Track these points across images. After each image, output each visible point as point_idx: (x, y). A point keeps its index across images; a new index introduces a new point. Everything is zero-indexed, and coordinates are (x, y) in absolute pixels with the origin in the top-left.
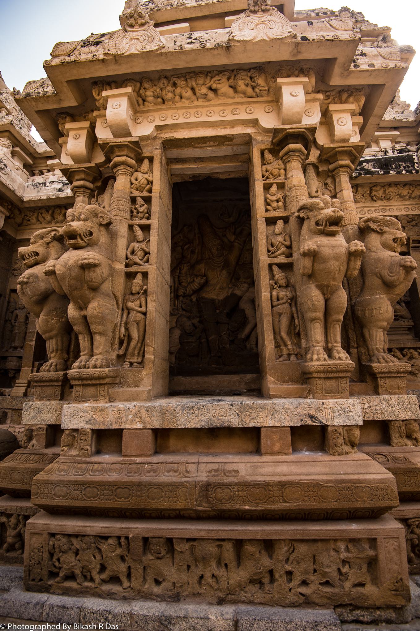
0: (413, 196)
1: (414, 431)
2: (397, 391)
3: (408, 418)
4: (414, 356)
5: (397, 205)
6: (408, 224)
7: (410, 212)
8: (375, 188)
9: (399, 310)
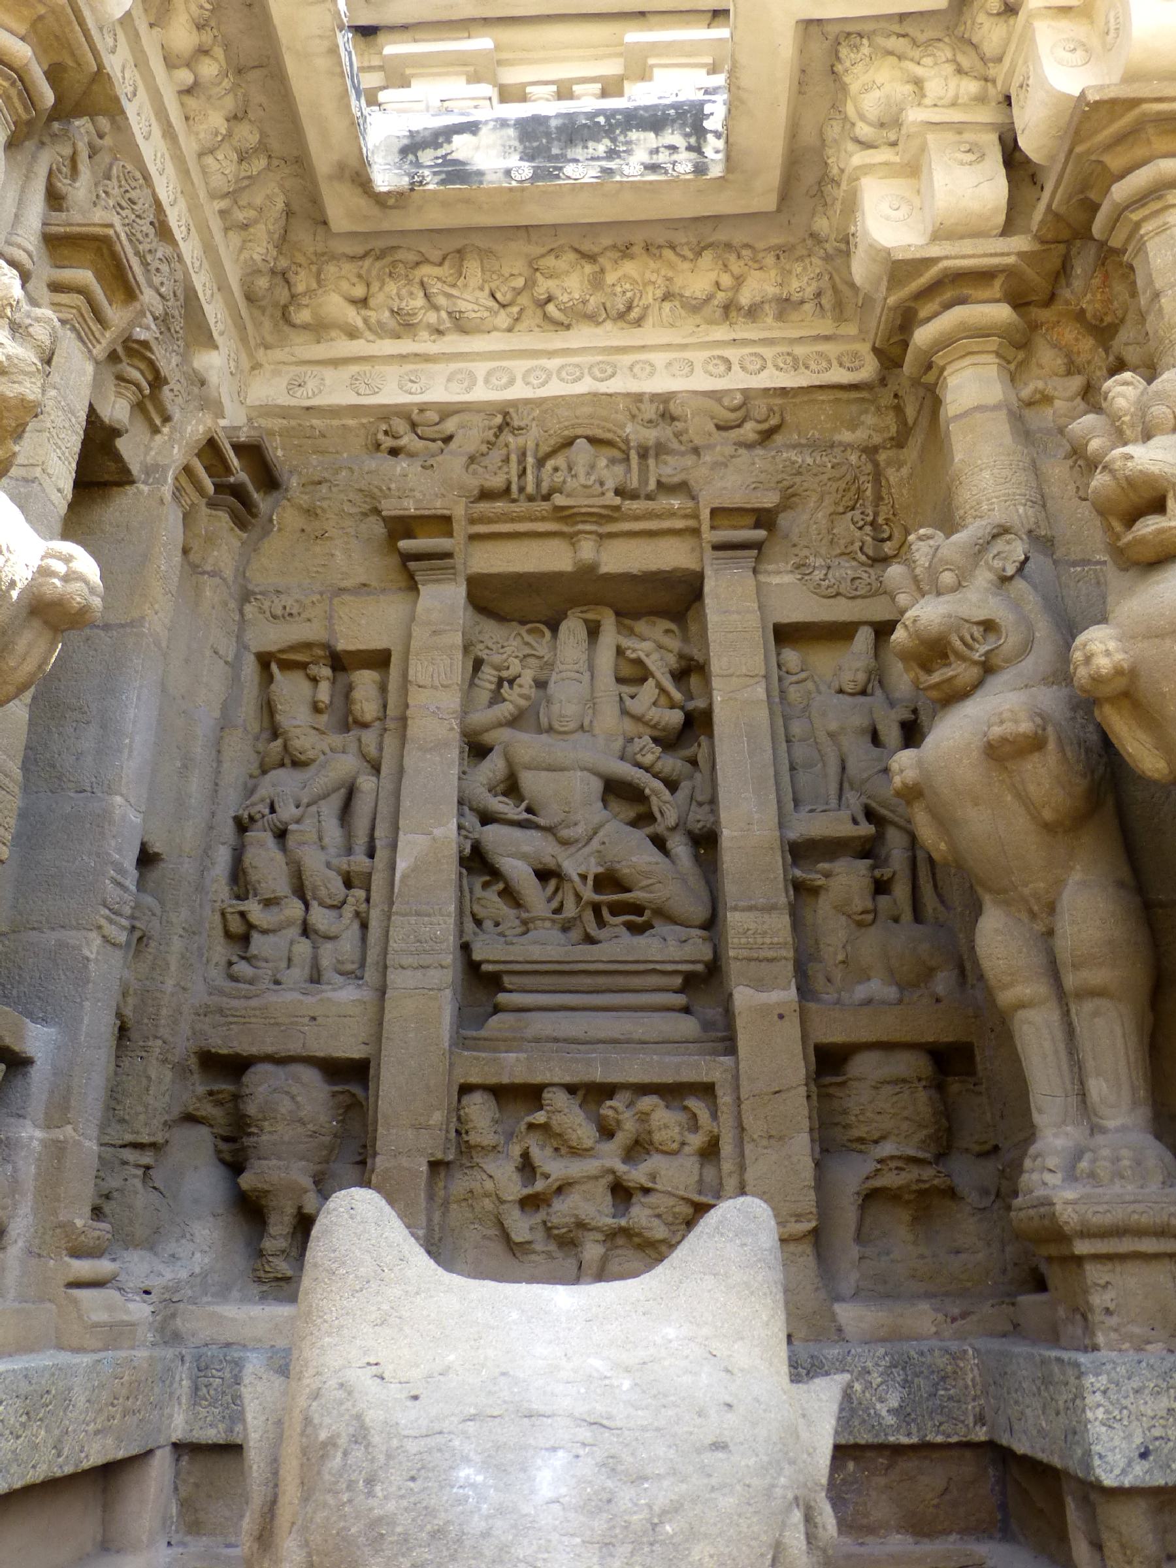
0: (745, 299)
4: (657, 1137)
5: (668, 347)
6: (718, 436)
7: (738, 381)
8: (550, 261)
9: (647, 875)
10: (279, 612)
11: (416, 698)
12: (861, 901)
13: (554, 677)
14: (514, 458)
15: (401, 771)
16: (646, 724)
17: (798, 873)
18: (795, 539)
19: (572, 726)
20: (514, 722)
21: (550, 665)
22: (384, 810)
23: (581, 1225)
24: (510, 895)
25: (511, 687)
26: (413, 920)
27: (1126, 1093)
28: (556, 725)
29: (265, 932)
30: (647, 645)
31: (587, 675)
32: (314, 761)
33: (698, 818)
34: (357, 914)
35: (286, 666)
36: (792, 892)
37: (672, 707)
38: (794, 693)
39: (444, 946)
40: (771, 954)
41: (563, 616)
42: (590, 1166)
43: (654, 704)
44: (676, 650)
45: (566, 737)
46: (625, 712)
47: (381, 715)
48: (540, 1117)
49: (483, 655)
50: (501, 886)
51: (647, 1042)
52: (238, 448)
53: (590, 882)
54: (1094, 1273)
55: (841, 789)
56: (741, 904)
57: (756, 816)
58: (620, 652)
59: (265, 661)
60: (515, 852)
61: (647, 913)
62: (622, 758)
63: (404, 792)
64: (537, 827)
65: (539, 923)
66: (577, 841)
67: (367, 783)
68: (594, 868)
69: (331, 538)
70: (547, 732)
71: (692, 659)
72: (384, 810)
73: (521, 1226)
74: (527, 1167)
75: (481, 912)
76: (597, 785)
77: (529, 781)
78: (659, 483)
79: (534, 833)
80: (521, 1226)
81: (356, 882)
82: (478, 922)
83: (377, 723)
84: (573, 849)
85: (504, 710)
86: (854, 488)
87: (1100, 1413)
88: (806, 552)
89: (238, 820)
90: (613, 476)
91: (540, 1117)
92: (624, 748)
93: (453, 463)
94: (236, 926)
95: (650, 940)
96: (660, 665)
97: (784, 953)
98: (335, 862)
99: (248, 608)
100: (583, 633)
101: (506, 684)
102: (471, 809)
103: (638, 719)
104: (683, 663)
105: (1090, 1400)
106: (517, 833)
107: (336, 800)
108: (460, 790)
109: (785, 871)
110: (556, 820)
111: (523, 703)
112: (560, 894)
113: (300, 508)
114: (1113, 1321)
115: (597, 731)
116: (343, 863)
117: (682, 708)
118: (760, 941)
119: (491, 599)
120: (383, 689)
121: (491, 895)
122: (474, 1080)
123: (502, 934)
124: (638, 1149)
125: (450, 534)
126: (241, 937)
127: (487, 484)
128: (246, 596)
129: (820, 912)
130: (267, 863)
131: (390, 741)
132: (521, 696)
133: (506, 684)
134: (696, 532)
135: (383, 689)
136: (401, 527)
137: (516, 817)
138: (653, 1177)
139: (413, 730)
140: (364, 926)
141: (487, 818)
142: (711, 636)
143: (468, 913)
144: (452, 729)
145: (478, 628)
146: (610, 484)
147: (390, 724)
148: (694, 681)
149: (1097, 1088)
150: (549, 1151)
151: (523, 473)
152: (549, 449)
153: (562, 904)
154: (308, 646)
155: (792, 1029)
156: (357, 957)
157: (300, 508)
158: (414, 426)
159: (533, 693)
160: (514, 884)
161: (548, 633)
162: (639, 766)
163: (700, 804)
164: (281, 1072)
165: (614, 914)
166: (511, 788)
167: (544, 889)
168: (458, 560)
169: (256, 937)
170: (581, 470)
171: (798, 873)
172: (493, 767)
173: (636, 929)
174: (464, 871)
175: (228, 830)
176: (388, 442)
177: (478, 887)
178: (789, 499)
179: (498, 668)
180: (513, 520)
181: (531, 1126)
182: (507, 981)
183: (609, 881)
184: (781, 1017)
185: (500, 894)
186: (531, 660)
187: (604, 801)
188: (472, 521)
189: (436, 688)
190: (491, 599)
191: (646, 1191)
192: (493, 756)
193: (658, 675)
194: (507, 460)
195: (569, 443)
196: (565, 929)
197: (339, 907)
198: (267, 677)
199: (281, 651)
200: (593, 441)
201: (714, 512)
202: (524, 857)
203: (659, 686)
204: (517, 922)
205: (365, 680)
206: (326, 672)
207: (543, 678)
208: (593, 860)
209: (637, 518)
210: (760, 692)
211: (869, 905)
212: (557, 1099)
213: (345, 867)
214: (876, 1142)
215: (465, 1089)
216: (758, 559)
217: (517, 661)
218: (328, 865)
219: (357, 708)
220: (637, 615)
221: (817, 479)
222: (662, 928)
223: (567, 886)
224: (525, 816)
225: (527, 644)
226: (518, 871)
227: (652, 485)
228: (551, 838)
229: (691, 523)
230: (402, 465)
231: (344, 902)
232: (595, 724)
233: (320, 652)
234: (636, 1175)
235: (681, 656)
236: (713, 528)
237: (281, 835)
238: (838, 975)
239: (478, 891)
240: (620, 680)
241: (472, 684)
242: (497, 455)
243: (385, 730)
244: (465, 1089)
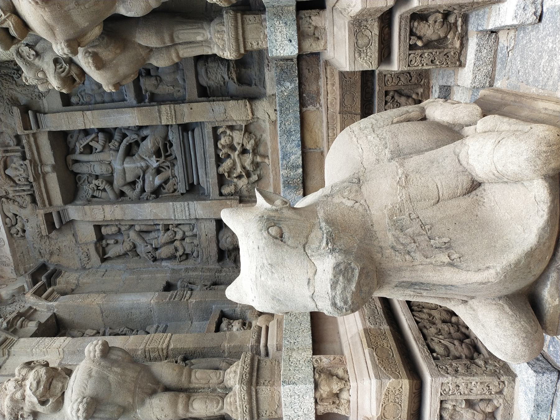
1: (331, 391)
2: (276, 397)
3: (313, 400)
4: (228, 143)
9: (154, 144)
10: (87, 259)
12: (153, 81)
14: (18, 194)
15: (132, 220)
17: (147, 100)
18: (29, 99)
19: (109, 167)
23: (253, 162)
24: (166, 181)
27: (201, 31)
28: (110, 172)
29: (185, 250)
30: (77, 145)
32: (133, 243)
35: (104, 253)
36: (154, 103)
37: (98, 136)
40: (173, 111)
41: (72, 171)
42: (237, 160)
43: (98, 142)
46: (102, 151)
48: (226, 174)
51: (204, 145)
52: (35, 282)
53: (159, 159)
54: (249, 48)
58: (81, 153)
59: (103, 260)
67: (137, 228)
68: (154, 158)
69: (59, 247)
73: (254, 178)
74: (240, 177)
76: (127, 159)
77: (129, 178)
78: (17, 145)
79: (146, 177)
80: (254, 178)
81: (167, 228)
82: (175, 190)
85: (107, 188)
86: (4, 77)
87: (282, 52)
88: (34, 95)
89: (154, 261)
90: (17, 162)
91: (226, 174)
93: (24, 213)
94: (184, 257)
97: (172, 107)
98: (162, 234)
99: (87, 267)
100: (77, 165)
103: (104, 147)
105: (279, 55)
106: (147, 182)
107: (144, 235)
110: (141, 170)
111: (104, 183)
113: (50, 257)
114: (260, 43)
116: (162, 232)
117: (98, 133)
119: (71, 194)
121: (167, 187)
122: (218, 193)
123: (178, 183)
124: (232, 148)
125: (51, 213)
126: (187, 256)
127: (30, 201)
128: (84, 268)
130: (164, 252)
132: (102, 184)
134: (34, 134)
136: (51, 226)
138: (239, 144)
140: (180, 224)
141: (143, 190)
146: (22, 162)
149: (199, 38)
150: (235, 171)
151: (24, 190)
152: (12, 182)
154: (97, 249)
155: (194, 105)
156: (188, 226)
157: (50, 257)
158: (12, 226)
161: (79, 175)
162: (119, 146)
164: (221, 241)
165: (167, 151)
166: (133, 184)
168: (59, 209)
169: (186, 252)
170: (18, 173)
171: (147, 100)
173: (171, 145)
175: (157, 263)
176: (21, 233)
177: (164, 191)
178: (14, 102)
179: (94, 191)
180: (42, 194)
181: (229, 176)
182: (191, 182)
183: (158, 154)
184: (191, 109)
186: (89, 180)
188: (45, 206)
190: (71, 194)
191: (243, 145)
192: (123, 190)
193: (87, 141)
194: (20, 196)
195: (9, 177)
196: (174, 165)
197: (175, 232)
198: (109, 259)
199: (100, 256)
200: (6, 167)
201: (26, 129)
203: (91, 141)
205: (104, 231)
206: (104, 242)
208: (152, 159)
209: (33, 153)
210: (88, 113)
211: (153, 79)
212: (221, 170)
214: (224, 79)
215: (221, 194)
216: (40, 112)
218: (163, 235)
220: (68, 147)
221: (4, 90)
223: (161, 165)
225: (84, 181)
226: (158, 181)
227: (18, 148)
229: (31, 136)
230: (27, 228)
233: (98, 245)
234: (239, 148)
236: (31, 129)
237: (156, 249)
238: (177, 89)
239: (166, 191)
242: (18, 199)
244: (221, 194)
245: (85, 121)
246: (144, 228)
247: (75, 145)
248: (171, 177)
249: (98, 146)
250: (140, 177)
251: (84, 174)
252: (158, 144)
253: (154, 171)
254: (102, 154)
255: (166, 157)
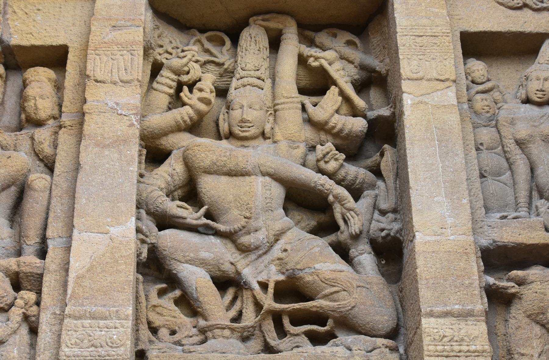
11: (94, 94)
13: (234, 83)
15: (77, 167)
16: (329, 132)
17: (491, 280)
19: (253, 131)
20: (194, 127)
21: (230, 73)
22: (58, 209)
24: (188, 304)
25: (191, 91)
26: (87, 322)
28: (237, 130)
30: (330, 54)
31: (269, 82)
33: (387, 225)
34: (26, 318)
36: (486, 300)
37: (355, 116)
38: (480, 102)
39: (121, 350)
41: (244, 24)
43: (337, 111)
44: (357, 62)
45: (246, 143)
47: (56, 112)
49: (162, 59)
50: (177, 293)
53: (271, 290)
55: (530, 197)
56: (439, 309)
57: (450, 221)
58: (302, 60)
60: (194, 256)
61: (330, 322)
62: (304, 165)
63: (79, 189)
64: (217, 233)
65: (217, 332)
66: (257, 248)
67: (39, 180)
68: (274, 276)
70: (227, 138)
71: (374, 71)
72: (58, 209)
75: (157, 321)
76: (278, 192)
77: (209, 186)
79: (213, 239)
81: (25, 284)
82: (154, 330)
83: (51, 122)
84: (253, 256)
85: (184, 114)
92: (306, 155)
95: (335, 349)
96: (343, 74)
100: (264, 42)
101: (185, 88)
102: (149, 213)
103: (319, 126)
104: (364, 74)
108: (139, 194)
109: (480, 277)
110: (236, 226)
111: (203, 107)
112: (238, 304)
115: (279, 136)
116: (12, 263)
117: (365, 117)
118: (457, 348)
120: (59, 88)
121: (167, 303)
129: (512, 321)
131: (64, 137)
132: (201, 100)
133: (185, 88)
135: (59, 88)
137: (195, 222)
139: (90, 126)
140: (34, 331)
141: (164, 222)
142: (401, 40)
143: (144, 320)
144: (132, 125)
145: (157, 32)
147: (66, 119)
148: (374, 94)
153: (240, 314)
159: (212, 97)
160: (192, 290)
161: (228, 42)
162: (321, 171)
163: (383, 213)
165: (295, 323)
166: (190, 194)
167: (222, 297)
171: (491, 280)
172: (172, 170)
173: (317, 339)
174: (140, 277)
177: (153, 293)
179: (178, 73)
183: (291, 289)
185: (177, 302)
186: (211, 67)
187: (285, 209)
189: (115, 83)
192: (171, 160)
196: (245, 339)
202: (202, 263)
203: (342, 93)
204: (195, 331)
205: (40, 78)
207: (222, 85)
208: (273, 268)
213: (15, 268)
217: (197, 66)
219: (30, 104)
220: (318, 28)
222: (345, 338)
223: (247, 294)
224: (205, 221)
226: (197, 279)
228: (230, 245)
231: (12, 305)
232: (277, 129)
235: (363, 67)
239: (154, 299)
240: (302, 91)
241: (150, 88)
243: (60, 127)
245: (424, 82)
246: (34, 206)
247: (324, 49)
248: (202, 323)
249: (327, 107)
250: (213, 220)
251: (235, 55)
252: (325, 297)
253: (227, 267)
254: (298, 116)
255: (277, 318)
